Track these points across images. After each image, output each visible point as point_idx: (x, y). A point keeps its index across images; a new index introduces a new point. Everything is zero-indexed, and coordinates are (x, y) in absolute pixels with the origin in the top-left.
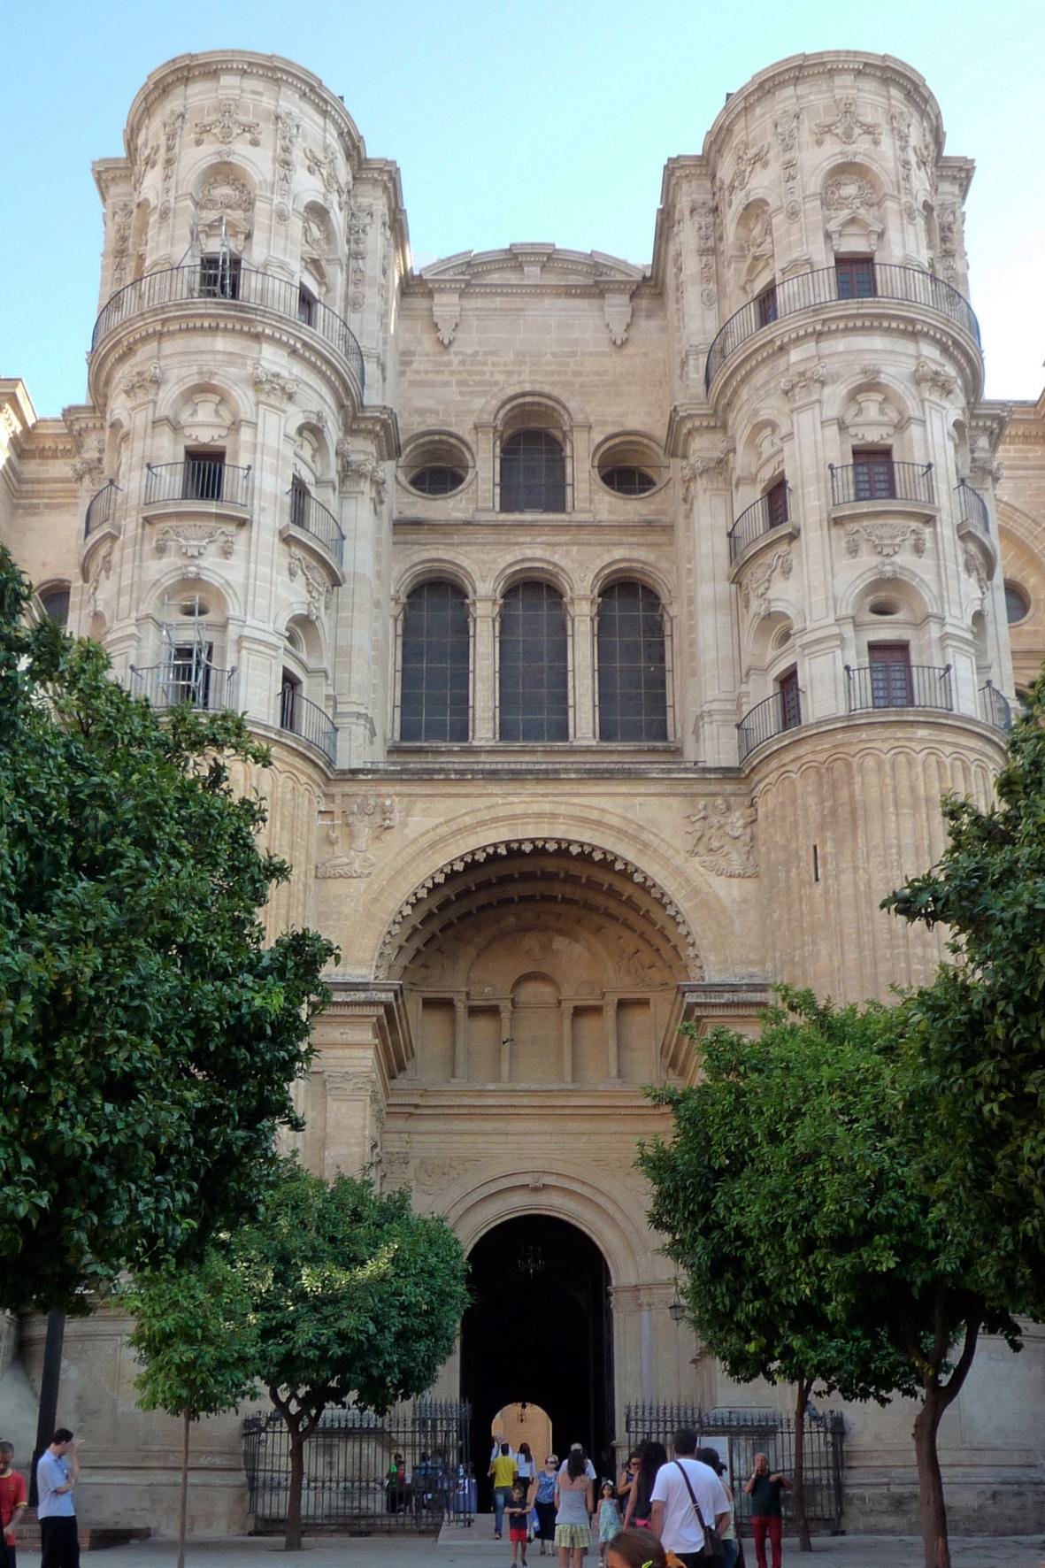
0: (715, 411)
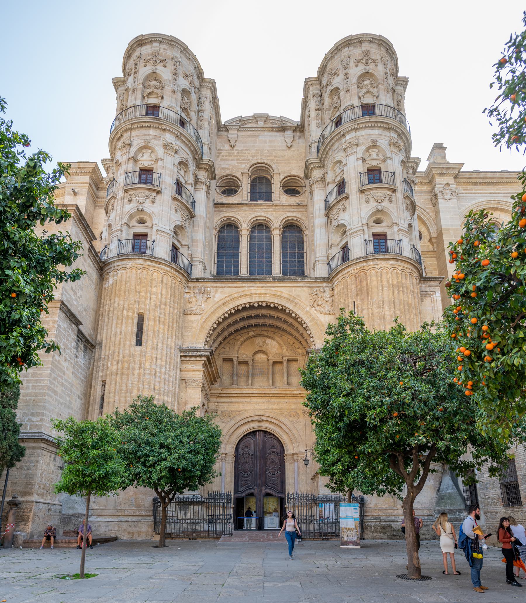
0: (321, 161)
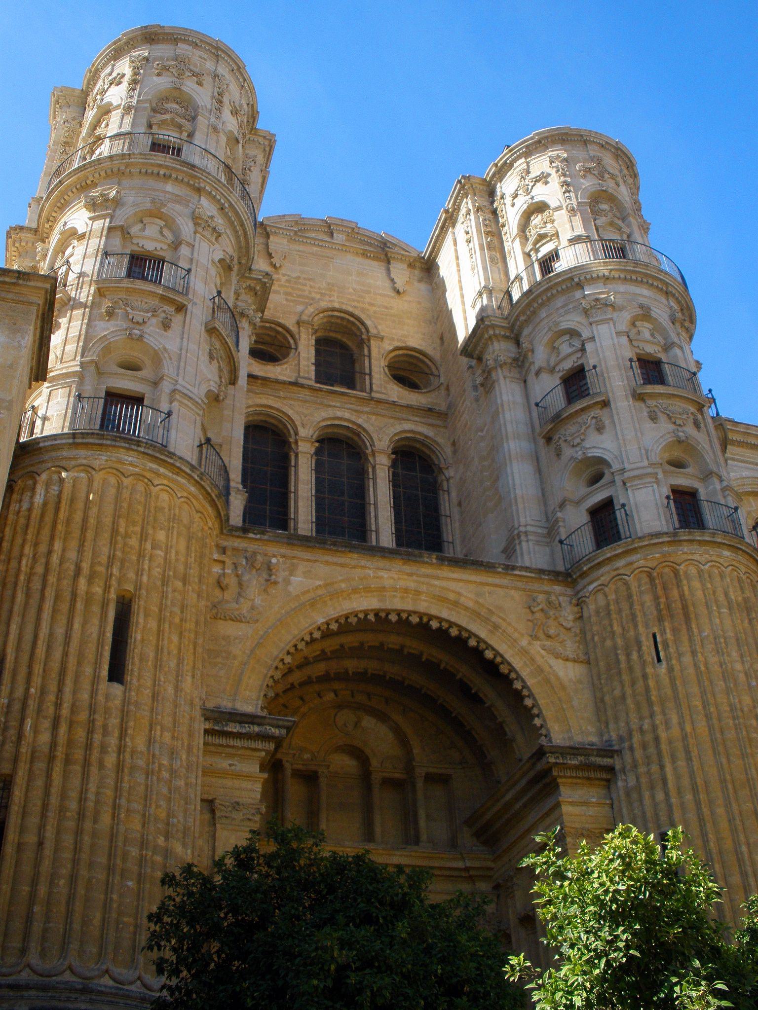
0: (513, 325)
